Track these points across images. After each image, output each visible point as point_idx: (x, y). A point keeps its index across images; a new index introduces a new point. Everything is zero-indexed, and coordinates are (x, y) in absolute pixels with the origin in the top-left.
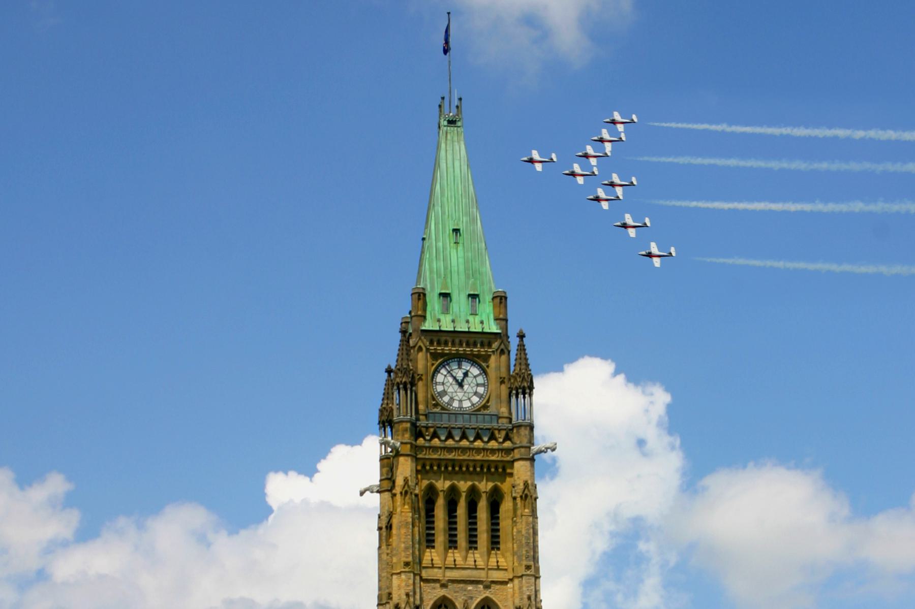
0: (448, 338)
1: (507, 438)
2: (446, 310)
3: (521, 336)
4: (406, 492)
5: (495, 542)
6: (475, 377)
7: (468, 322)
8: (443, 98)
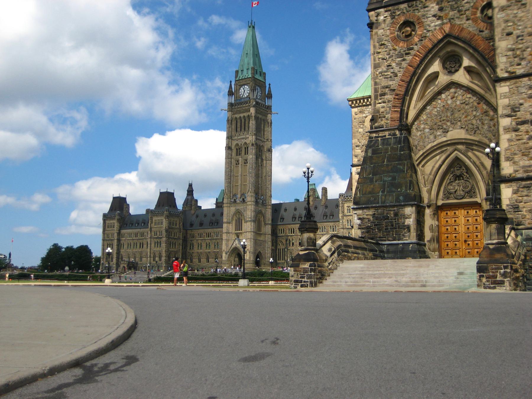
2: (242, 74)
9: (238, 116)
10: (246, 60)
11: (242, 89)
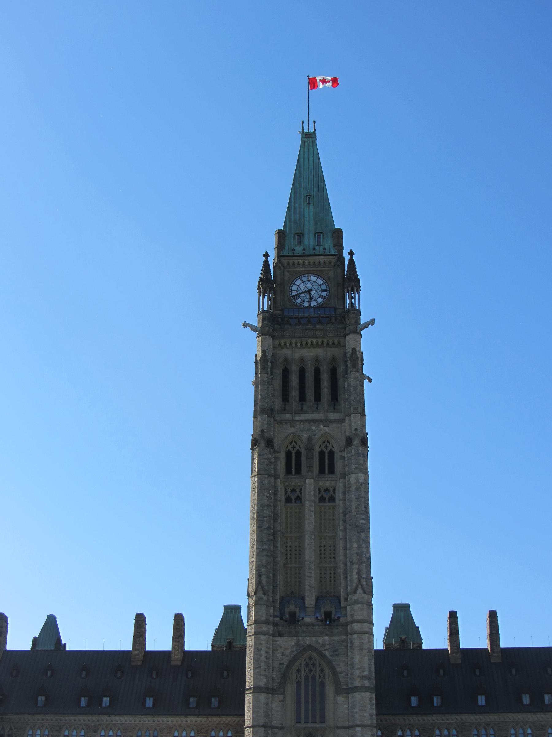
0: (300, 261)
2: (299, 243)
3: (351, 253)
5: (334, 396)
6: (320, 285)
7: (314, 249)
8: (303, 122)
10: (308, 213)
11: (298, 282)
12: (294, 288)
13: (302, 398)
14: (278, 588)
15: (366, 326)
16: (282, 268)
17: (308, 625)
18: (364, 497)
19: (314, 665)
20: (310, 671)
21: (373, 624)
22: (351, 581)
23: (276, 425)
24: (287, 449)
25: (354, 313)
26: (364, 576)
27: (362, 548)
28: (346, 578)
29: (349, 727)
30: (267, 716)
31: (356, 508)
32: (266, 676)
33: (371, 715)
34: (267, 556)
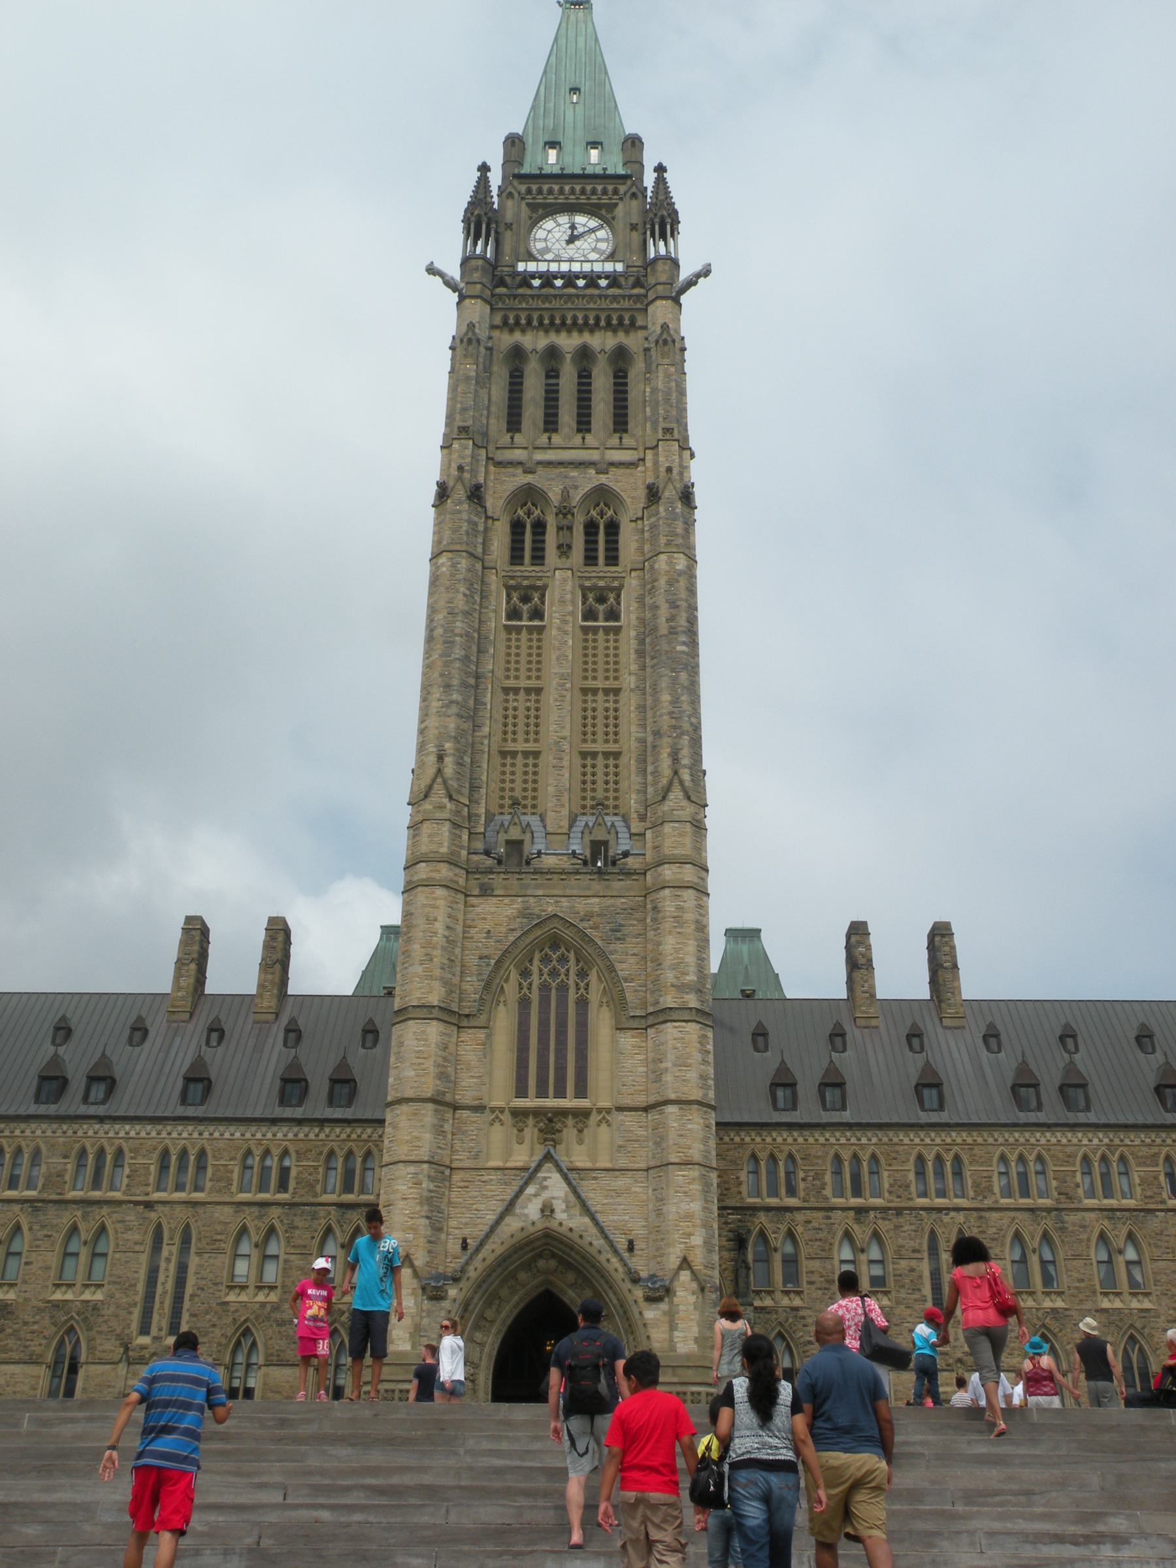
1: (638, 283)
3: (660, 169)
4: (470, 341)
5: (620, 423)
9: (534, 341)
11: (549, 224)
12: (540, 234)
13: (551, 423)
14: (483, 791)
15: (691, 283)
16: (516, 195)
17: (550, 872)
18: (687, 601)
19: (563, 960)
20: (554, 973)
21: (707, 871)
22: (655, 773)
23: (492, 468)
24: (515, 517)
25: (665, 264)
26: (685, 761)
27: (682, 702)
28: (643, 772)
29: (646, 1109)
30: (442, 1076)
31: (668, 620)
32: (446, 983)
33: (703, 1077)
34: (459, 716)
